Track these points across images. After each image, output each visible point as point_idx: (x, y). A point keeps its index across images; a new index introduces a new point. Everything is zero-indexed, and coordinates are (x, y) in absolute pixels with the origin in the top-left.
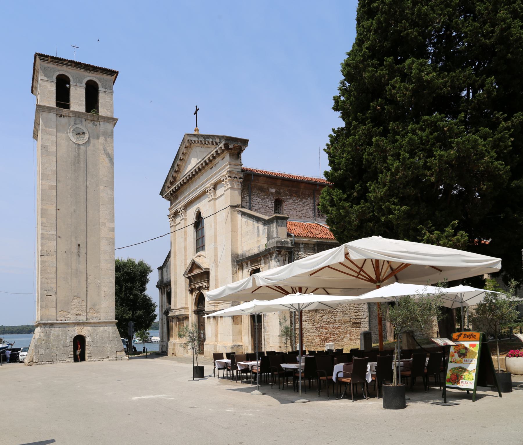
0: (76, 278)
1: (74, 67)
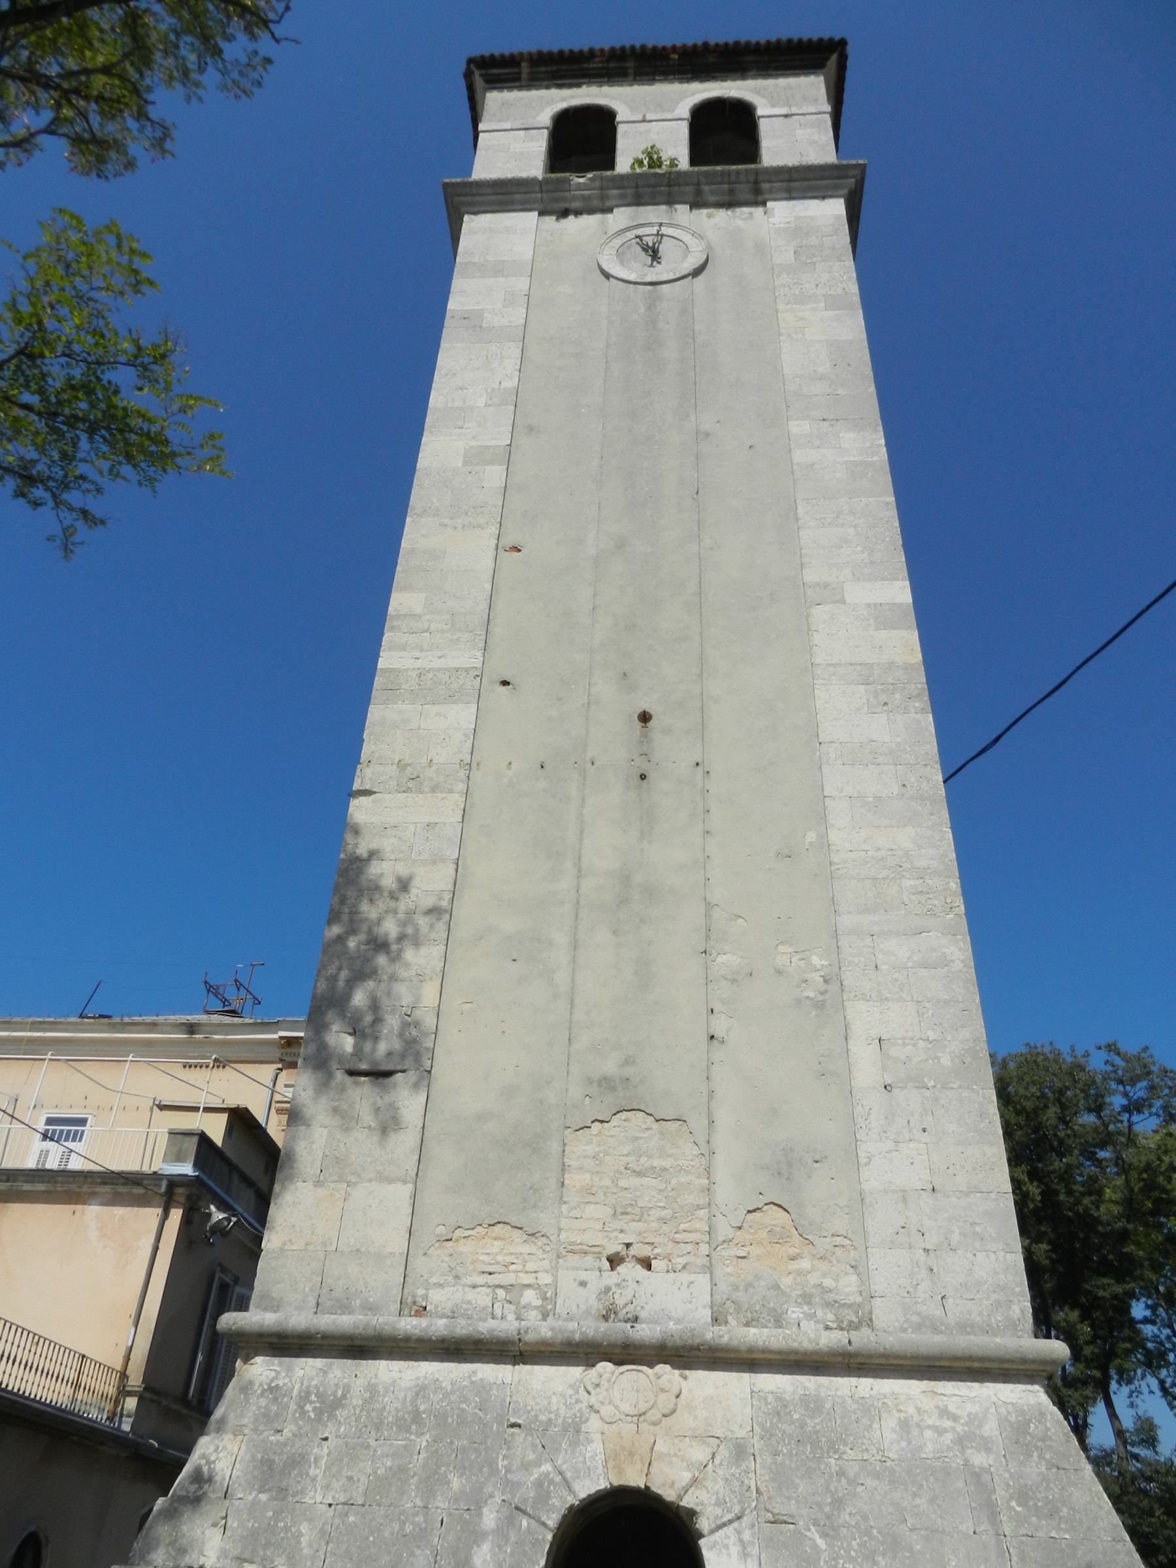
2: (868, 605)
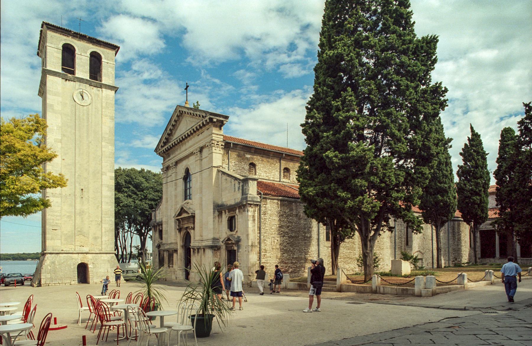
1: (80, 38)
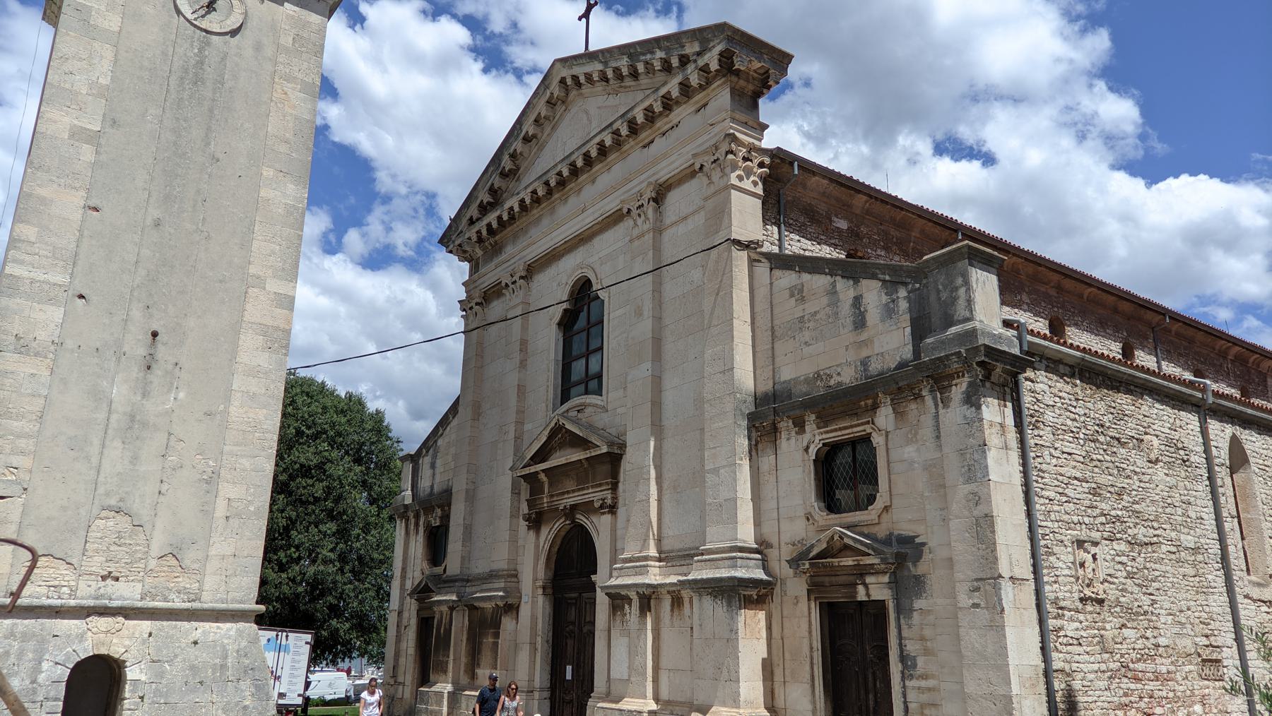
0: (123, 443)
2: (275, 293)
